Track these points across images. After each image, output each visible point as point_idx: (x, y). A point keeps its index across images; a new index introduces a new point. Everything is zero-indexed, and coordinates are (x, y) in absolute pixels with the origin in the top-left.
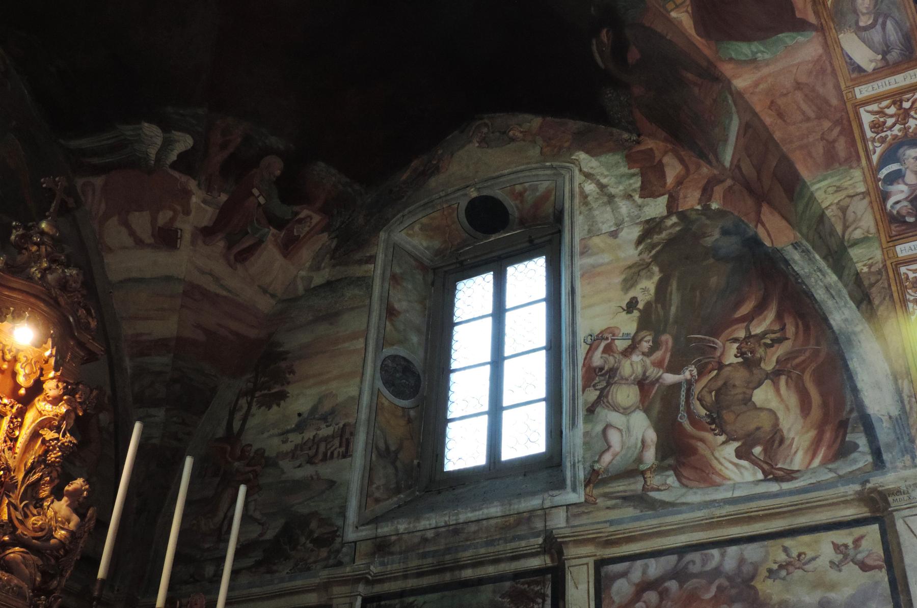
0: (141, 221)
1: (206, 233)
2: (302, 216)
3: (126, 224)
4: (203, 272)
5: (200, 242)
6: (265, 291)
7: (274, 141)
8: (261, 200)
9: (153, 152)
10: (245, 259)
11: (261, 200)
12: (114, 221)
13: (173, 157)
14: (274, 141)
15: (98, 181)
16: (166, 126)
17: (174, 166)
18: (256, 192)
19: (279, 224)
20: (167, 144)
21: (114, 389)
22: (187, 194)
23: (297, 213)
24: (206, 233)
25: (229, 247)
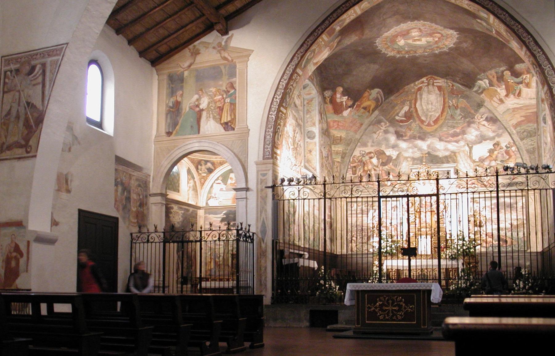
0: (495, 99)
1: (507, 96)
2: (524, 77)
3: (494, 101)
4: (513, 104)
5: (507, 98)
6: (531, 99)
7: (502, 69)
8: (512, 81)
9: (484, 85)
10: (520, 95)
11: (512, 81)
12: (492, 102)
13: (488, 85)
14: (502, 69)
15: (483, 95)
16: (481, 80)
17: (490, 86)
18: (509, 80)
19: (521, 83)
20: (485, 83)
21: (513, 140)
22: (496, 91)
23: (523, 78)
24: (507, 96)
25: (514, 95)
